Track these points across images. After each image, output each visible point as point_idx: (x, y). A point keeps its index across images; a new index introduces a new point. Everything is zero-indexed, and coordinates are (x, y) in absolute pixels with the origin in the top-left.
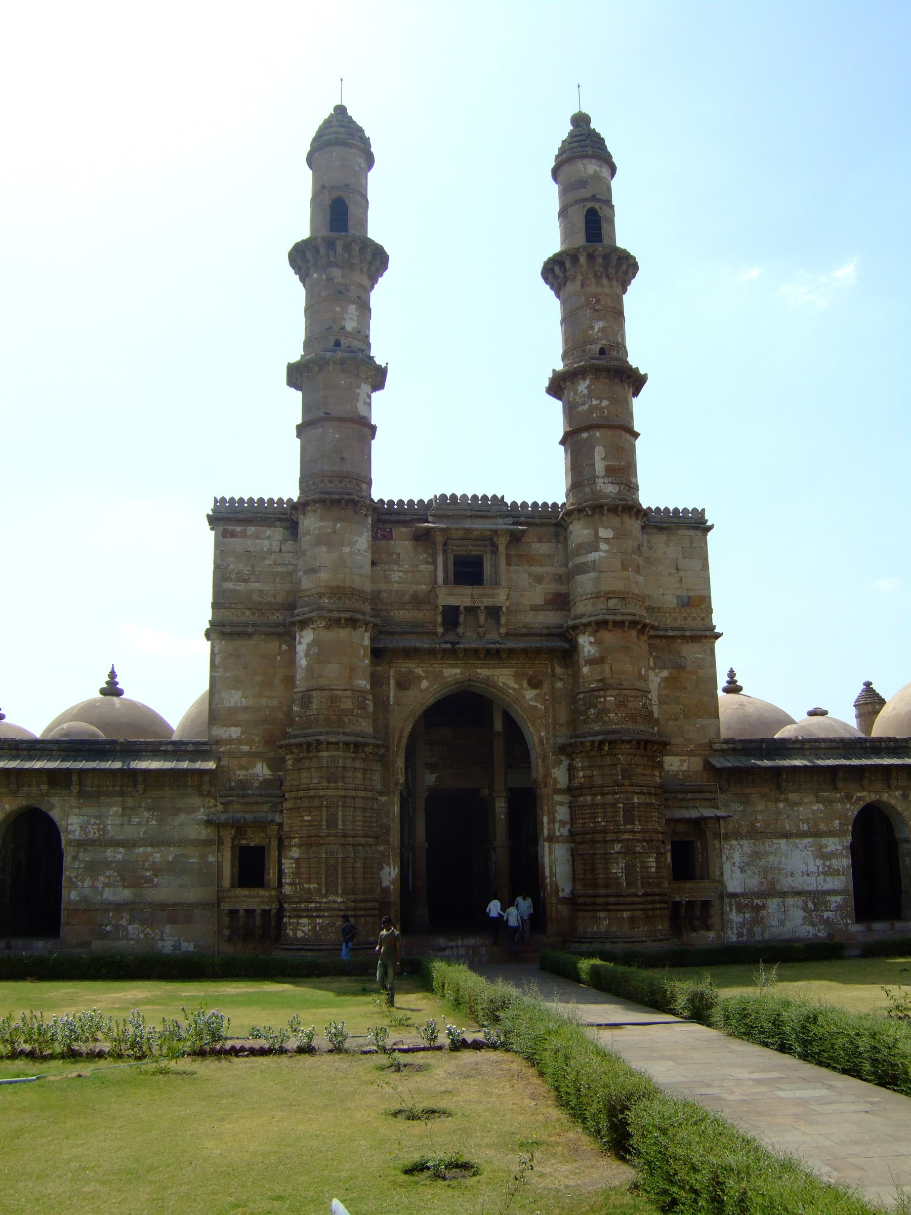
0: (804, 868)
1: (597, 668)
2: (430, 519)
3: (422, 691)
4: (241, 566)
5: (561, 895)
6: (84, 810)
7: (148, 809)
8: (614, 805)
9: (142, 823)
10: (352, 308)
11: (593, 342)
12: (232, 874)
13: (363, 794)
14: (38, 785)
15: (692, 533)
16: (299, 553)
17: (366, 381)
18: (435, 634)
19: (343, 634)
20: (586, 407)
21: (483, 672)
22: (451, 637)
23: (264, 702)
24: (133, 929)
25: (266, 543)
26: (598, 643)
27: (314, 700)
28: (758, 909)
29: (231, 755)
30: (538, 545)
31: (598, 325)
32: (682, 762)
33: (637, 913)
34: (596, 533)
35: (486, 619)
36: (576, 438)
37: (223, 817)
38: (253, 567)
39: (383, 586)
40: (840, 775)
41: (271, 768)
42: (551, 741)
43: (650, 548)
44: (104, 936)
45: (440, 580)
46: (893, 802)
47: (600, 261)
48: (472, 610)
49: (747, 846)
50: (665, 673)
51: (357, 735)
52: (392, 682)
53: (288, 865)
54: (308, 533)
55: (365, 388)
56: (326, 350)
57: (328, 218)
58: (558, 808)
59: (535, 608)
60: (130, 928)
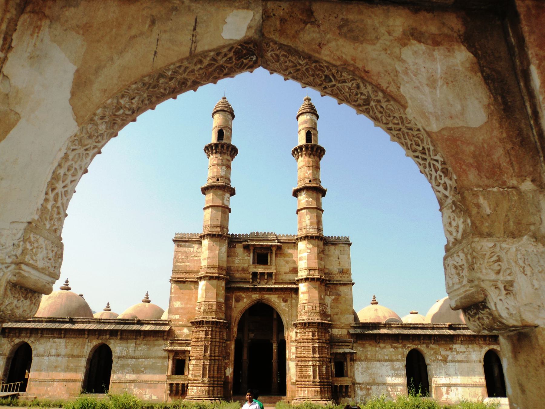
4: (183, 257)
6: (122, 345)
7: (144, 345)
9: (143, 349)
12: (173, 369)
13: (218, 340)
14: (106, 335)
15: (344, 245)
17: (227, 192)
18: (249, 282)
19: (215, 282)
21: (266, 296)
22: (255, 283)
25: (192, 249)
32: (339, 331)
35: (268, 277)
36: (301, 212)
37: (170, 348)
39: (232, 265)
40: (400, 338)
41: (189, 330)
46: (422, 349)
48: (262, 274)
49: (364, 364)
50: (333, 297)
52: (234, 299)
53: (191, 367)
55: (227, 195)
56: (214, 182)
58: (292, 347)
59: (285, 273)
60: (134, 390)
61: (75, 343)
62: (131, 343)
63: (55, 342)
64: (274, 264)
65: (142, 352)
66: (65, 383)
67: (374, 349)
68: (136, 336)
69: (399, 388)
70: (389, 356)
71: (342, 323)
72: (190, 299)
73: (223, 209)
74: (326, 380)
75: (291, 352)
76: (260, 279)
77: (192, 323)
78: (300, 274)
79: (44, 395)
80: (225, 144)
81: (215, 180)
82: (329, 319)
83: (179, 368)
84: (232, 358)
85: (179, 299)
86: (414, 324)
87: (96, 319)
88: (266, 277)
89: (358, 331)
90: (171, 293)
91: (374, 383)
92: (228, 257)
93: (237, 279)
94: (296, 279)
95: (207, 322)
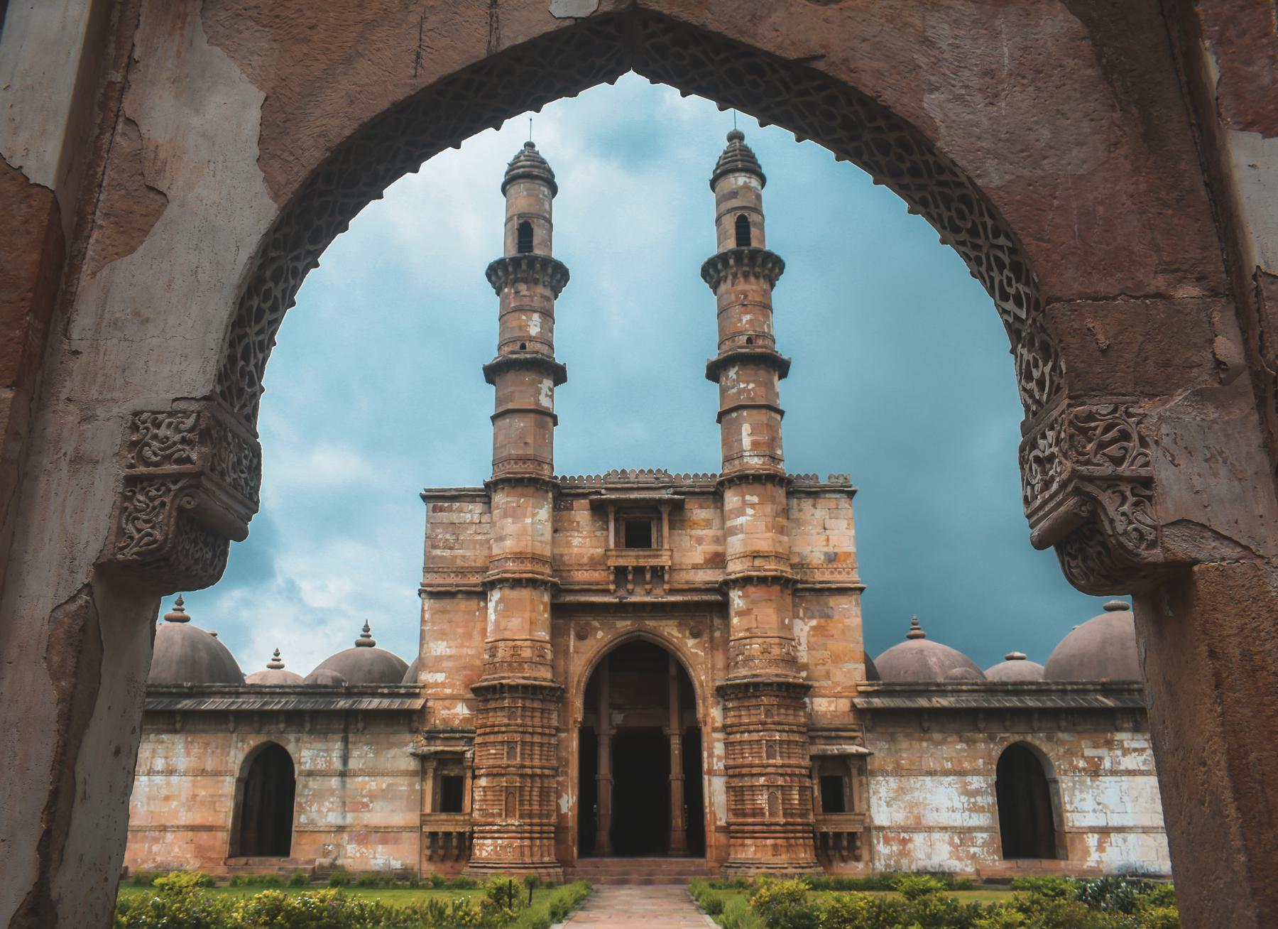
0: (950, 805)
1: (745, 619)
2: (603, 491)
3: (598, 641)
5: (719, 823)
7: (367, 744)
8: (758, 742)
9: (361, 756)
11: (741, 333)
15: (837, 496)
16: (492, 523)
19: (525, 593)
20: (735, 390)
21: (651, 624)
22: (622, 593)
23: (465, 651)
24: (351, 849)
26: (744, 597)
28: (904, 842)
29: (438, 698)
30: (699, 511)
33: (779, 841)
34: (744, 501)
35: (652, 577)
36: (728, 417)
39: (565, 551)
41: (469, 708)
42: (710, 684)
43: (800, 510)
44: (326, 854)
45: (612, 545)
46: (1037, 743)
48: (639, 571)
49: (893, 782)
50: (814, 623)
51: (535, 679)
59: (696, 567)
60: (349, 847)
61: (207, 744)
62: (334, 741)
63: (163, 742)
64: (666, 546)
66: (190, 833)
67: (916, 745)
69: (981, 837)
70: (955, 762)
71: (836, 684)
72: (468, 635)
73: (539, 417)
74: (799, 820)
75: (715, 752)
76: (634, 582)
77: (474, 690)
79: (143, 862)
81: (517, 347)
82: (804, 674)
83: (450, 796)
84: (574, 770)
85: (442, 635)
86: (1015, 684)
87: (252, 685)
88: (648, 576)
89: (877, 702)
90: (423, 621)
91: (918, 827)
92: (555, 531)
93: (579, 583)
94: (720, 579)
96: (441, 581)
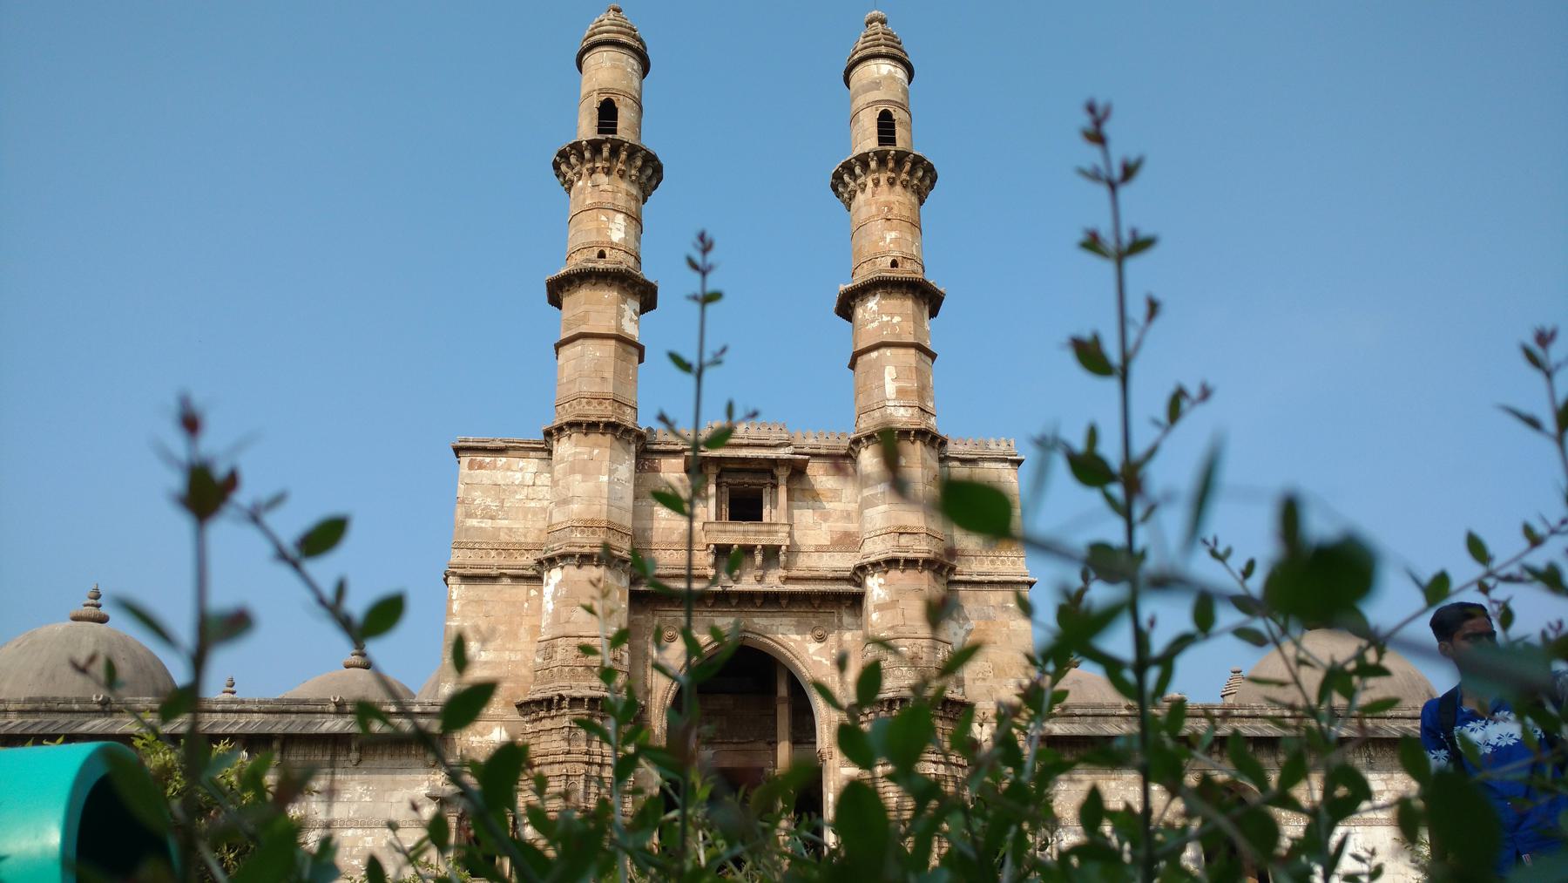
1: (889, 614)
4: (489, 501)
7: (363, 783)
10: (620, 218)
20: (876, 324)
21: (760, 622)
23: (506, 655)
25: (518, 475)
26: (887, 585)
27: (559, 650)
31: (891, 235)
36: (866, 358)
38: (502, 502)
45: (713, 518)
47: (891, 165)
48: (748, 550)
54: (562, 461)
57: (596, 122)
59: (820, 549)
65: (355, 806)
68: (333, 756)
77: (519, 706)
78: (868, 547)
80: (622, 143)
88: (759, 559)
92: (636, 498)
95: (575, 701)
96: (478, 561)
